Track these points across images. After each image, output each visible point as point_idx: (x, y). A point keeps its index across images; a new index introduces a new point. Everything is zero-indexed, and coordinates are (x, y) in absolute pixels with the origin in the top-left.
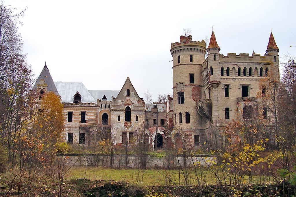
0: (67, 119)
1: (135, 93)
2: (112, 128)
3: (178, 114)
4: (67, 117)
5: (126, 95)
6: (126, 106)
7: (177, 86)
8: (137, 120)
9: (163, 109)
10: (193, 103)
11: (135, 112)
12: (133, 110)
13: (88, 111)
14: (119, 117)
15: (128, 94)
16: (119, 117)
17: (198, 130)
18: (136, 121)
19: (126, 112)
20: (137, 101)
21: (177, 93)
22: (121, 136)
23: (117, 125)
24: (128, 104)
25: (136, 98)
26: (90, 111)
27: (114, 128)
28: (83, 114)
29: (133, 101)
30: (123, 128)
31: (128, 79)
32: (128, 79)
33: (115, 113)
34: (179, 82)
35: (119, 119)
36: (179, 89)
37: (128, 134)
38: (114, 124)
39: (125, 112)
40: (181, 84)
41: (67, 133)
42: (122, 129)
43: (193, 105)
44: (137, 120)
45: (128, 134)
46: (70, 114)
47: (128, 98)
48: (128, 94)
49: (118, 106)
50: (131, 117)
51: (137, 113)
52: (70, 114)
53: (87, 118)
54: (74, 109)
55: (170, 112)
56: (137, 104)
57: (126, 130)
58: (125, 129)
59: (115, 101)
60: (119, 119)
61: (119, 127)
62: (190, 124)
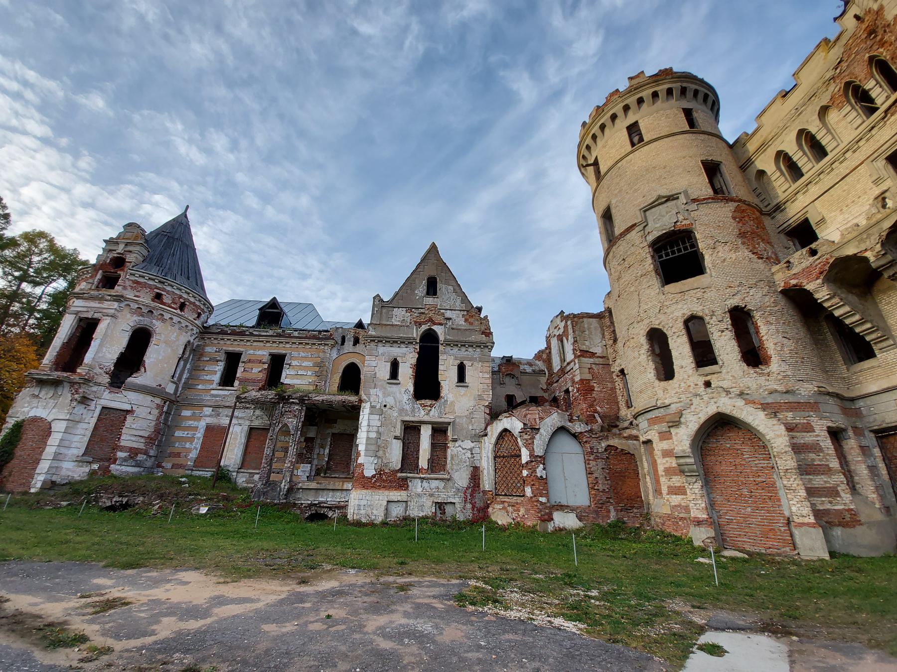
0: (217, 378)
1: (457, 288)
2: (363, 405)
3: (680, 325)
4: (220, 368)
5: (425, 292)
6: (424, 327)
7: (646, 217)
8: (461, 377)
9: (531, 369)
10: (755, 266)
11: (456, 350)
12: (448, 343)
13: (295, 354)
14: (395, 366)
15: (432, 288)
16: (395, 366)
17: (831, 401)
18: (461, 384)
19: (420, 346)
20: (462, 313)
21: (646, 244)
22: (396, 438)
23: (385, 395)
24: (431, 320)
25: (458, 304)
26: (302, 354)
27: (372, 407)
28: (277, 363)
29: (448, 314)
30: (408, 407)
31: (434, 247)
32: (434, 247)
33: (381, 349)
34: (659, 197)
35: (394, 374)
36: (658, 225)
37: (426, 433)
38: (373, 391)
39: (418, 347)
40: (669, 204)
41: (202, 424)
42: (402, 411)
43: (762, 277)
44: (461, 377)
45: (426, 433)
46: (233, 360)
47: (430, 300)
48: (432, 288)
49: (392, 325)
50: (441, 367)
51: (463, 353)
52: (233, 360)
53: (287, 377)
54: (249, 343)
55: (579, 356)
56: (461, 322)
57: (421, 414)
58: (413, 411)
59: (384, 311)
60: (394, 374)
61: (390, 401)
62: (775, 366)
